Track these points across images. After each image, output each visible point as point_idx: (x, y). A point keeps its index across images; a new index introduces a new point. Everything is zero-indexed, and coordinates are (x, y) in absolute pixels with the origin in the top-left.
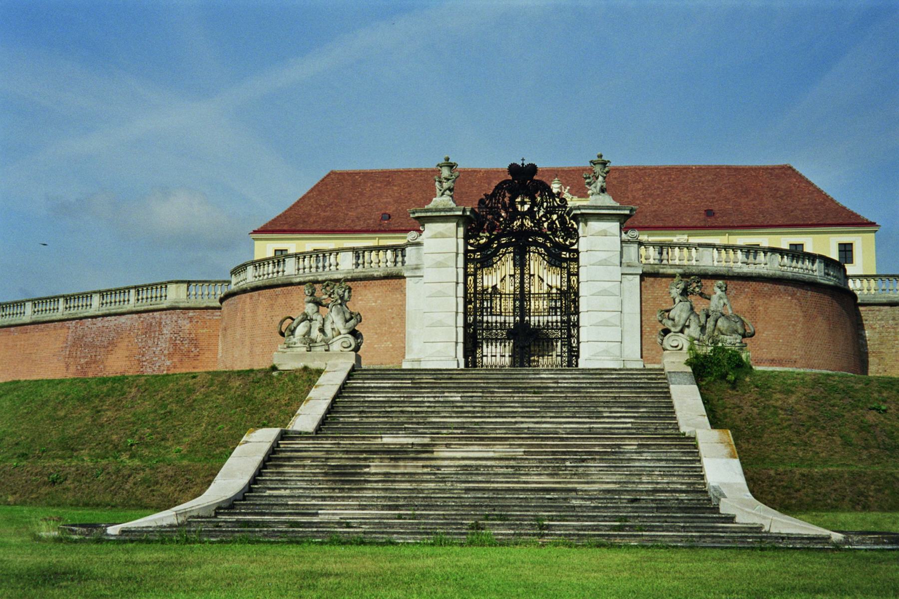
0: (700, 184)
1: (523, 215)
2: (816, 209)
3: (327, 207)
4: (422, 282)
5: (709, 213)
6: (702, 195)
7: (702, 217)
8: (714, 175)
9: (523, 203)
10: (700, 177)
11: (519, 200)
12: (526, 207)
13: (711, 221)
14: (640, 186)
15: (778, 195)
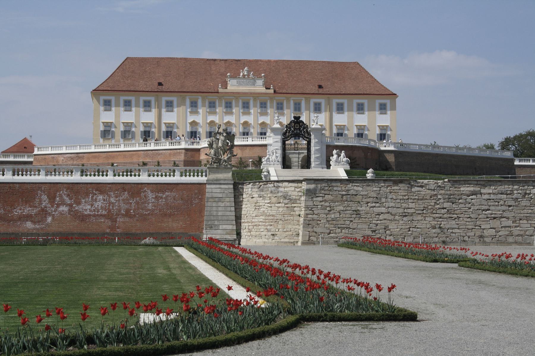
0: (315, 71)
1: (297, 129)
2: (370, 86)
3: (128, 78)
4: (272, 146)
5: (320, 87)
6: (316, 77)
7: (317, 88)
8: (322, 66)
9: (297, 126)
10: (315, 67)
11: (296, 125)
12: (298, 127)
13: (321, 91)
14: (286, 71)
15: (352, 78)
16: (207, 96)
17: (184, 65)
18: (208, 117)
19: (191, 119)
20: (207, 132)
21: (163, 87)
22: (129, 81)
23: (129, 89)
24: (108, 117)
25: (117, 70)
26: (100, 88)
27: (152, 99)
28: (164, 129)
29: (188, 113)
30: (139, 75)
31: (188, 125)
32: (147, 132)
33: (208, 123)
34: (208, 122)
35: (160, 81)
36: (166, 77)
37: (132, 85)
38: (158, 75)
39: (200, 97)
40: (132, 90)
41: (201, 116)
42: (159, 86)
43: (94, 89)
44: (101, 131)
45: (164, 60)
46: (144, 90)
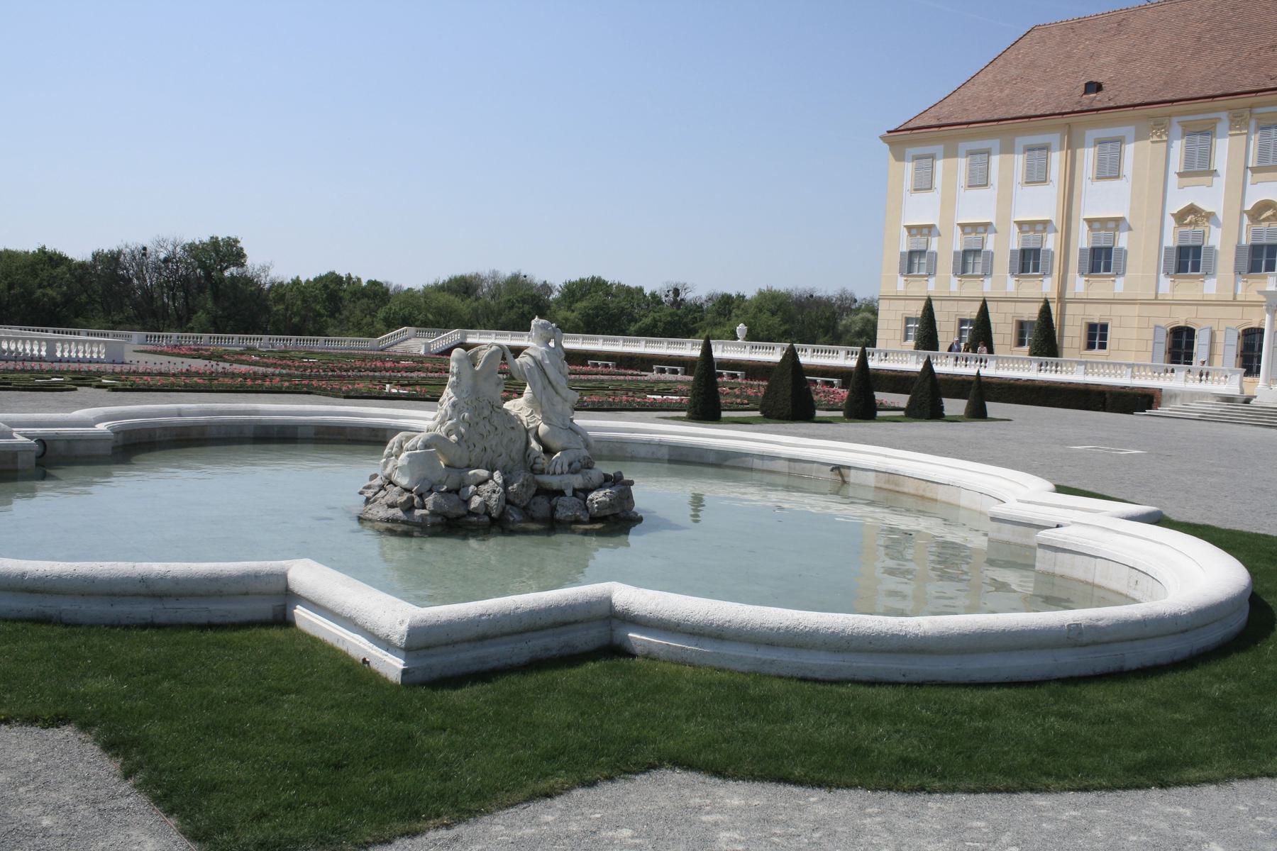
16: (1251, 107)
17: (1208, 15)
18: (1249, 187)
19: (1178, 200)
20: (1239, 248)
21: (1100, 95)
22: (1007, 92)
23: (988, 117)
24: (921, 209)
25: (990, 66)
26: (910, 125)
27: (1054, 138)
28: (1083, 239)
29: (1173, 179)
30: (1045, 71)
31: (1170, 223)
32: (1032, 254)
33: (1246, 212)
34: (1248, 207)
35: (1100, 80)
36: (1128, 62)
37: (1005, 104)
38: (1102, 61)
39: (1224, 115)
40: (996, 117)
41: (1220, 182)
42: (1084, 96)
43: (892, 129)
44: (902, 254)
45: (1144, 11)
46: (1032, 113)
